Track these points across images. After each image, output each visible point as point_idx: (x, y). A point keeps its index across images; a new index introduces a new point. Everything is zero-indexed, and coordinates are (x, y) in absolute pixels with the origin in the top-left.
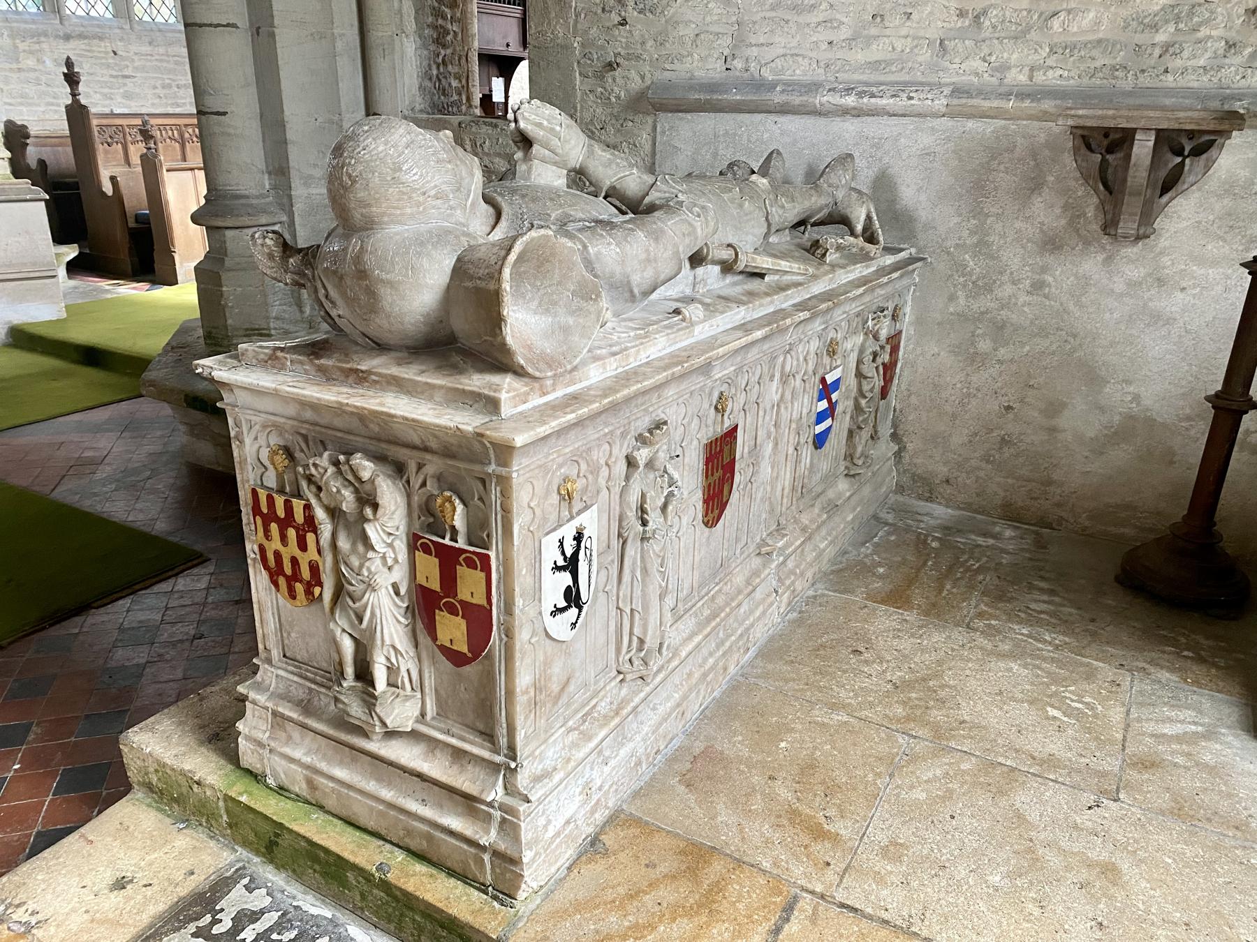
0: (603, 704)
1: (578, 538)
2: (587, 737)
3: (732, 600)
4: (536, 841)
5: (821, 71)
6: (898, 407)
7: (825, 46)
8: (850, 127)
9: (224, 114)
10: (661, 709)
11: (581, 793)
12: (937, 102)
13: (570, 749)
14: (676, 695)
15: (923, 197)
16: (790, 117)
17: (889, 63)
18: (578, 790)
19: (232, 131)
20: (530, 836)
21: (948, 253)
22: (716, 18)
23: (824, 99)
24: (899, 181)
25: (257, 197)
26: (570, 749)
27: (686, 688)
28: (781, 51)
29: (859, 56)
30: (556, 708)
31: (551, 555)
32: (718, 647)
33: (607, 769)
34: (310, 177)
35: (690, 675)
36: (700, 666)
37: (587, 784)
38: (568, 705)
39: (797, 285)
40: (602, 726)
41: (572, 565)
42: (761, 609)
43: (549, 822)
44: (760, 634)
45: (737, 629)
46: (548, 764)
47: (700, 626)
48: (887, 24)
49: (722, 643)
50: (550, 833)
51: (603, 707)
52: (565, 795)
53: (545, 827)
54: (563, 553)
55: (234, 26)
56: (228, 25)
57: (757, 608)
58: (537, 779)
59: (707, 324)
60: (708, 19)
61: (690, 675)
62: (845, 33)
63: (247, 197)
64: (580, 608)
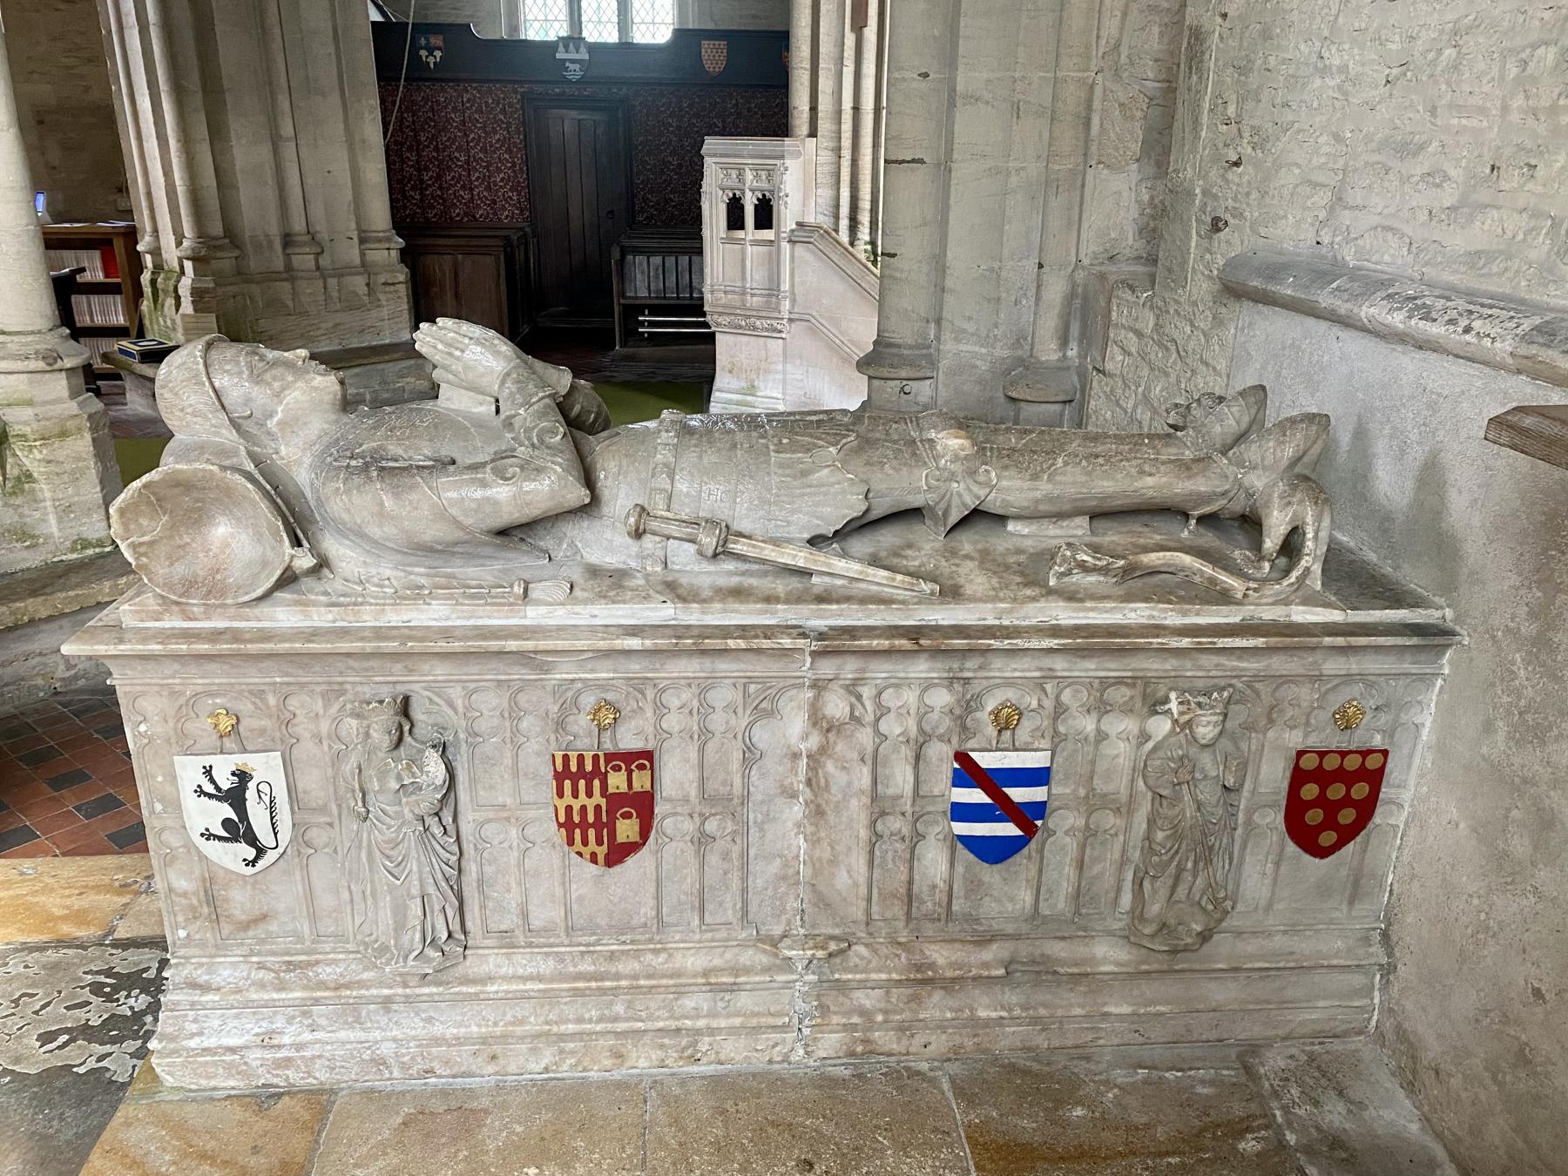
0: (328, 970)
1: (243, 777)
2: (281, 986)
3: (649, 977)
4: (172, 1039)
5: (1410, 259)
6: (1395, 887)
7: (1423, 217)
8: (1409, 363)
9: (894, 255)
10: (437, 1030)
11: (257, 1035)
12: (1498, 345)
13: (253, 984)
14: (475, 1029)
15: (1476, 521)
16: (1355, 334)
17: (1490, 256)
18: (257, 1030)
19: (898, 275)
20: (170, 1030)
21: (1493, 637)
22: (1323, 160)
23: (1373, 311)
24: (1451, 477)
25: (911, 347)
26: (253, 984)
27: (498, 1030)
28: (1376, 220)
29: (1458, 241)
30: (242, 935)
31: (189, 772)
32: (600, 1020)
33: (307, 1036)
34: (964, 331)
35: (522, 1022)
36: (547, 1023)
37: (273, 1032)
38: (262, 941)
39: (865, 600)
40: (306, 988)
41: (235, 796)
42: (737, 1021)
43: (200, 1034)
44: (737, 1054)
45: (658, 1019)
46: (216, 980)
47: (561, 977)
48: (1503, 185)
49: (615, 1019)
50: (193, 1043)
51: (326, 973)
52: (236, 1023)
53: (193, 1035)
54: (212, 781)
55: (921, 161)
56: (913, 161)
57: (729, 1016)
58: (193, 985)
59: (561, 611)
60: (1315, 161)
61: (522, 1022)
62: (1449, 196)
63: (899, 346)
64: (261, 851)
